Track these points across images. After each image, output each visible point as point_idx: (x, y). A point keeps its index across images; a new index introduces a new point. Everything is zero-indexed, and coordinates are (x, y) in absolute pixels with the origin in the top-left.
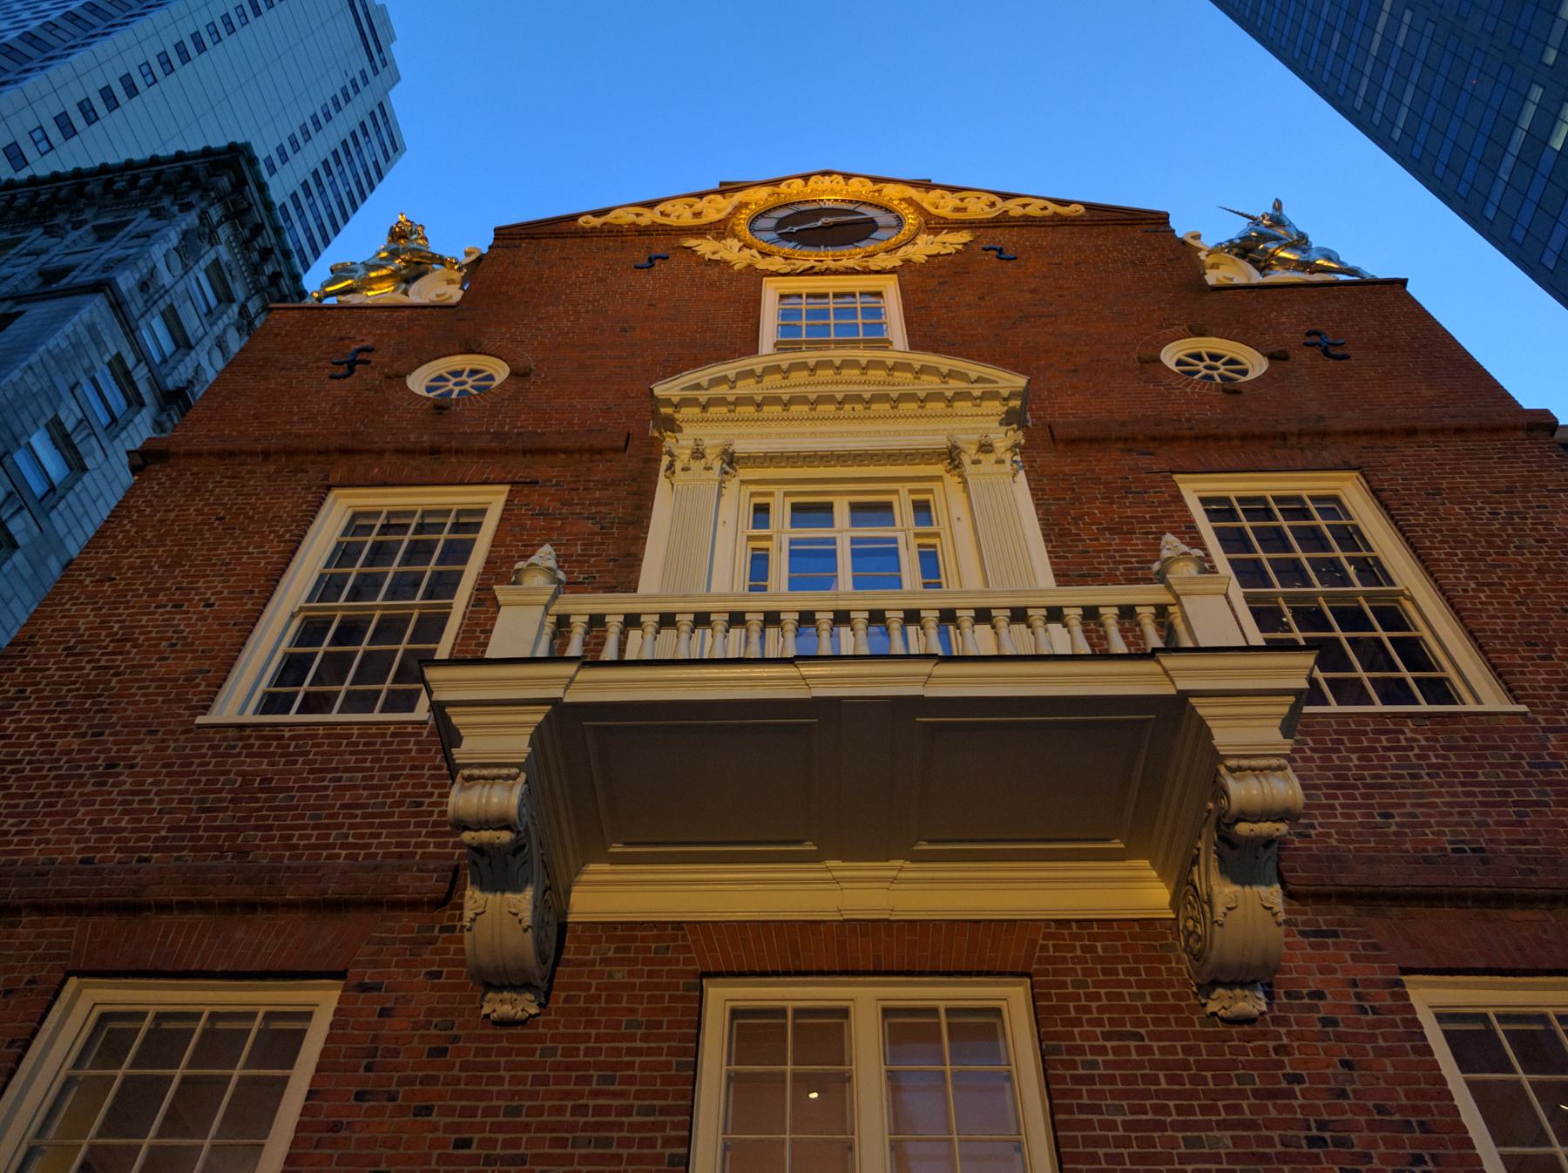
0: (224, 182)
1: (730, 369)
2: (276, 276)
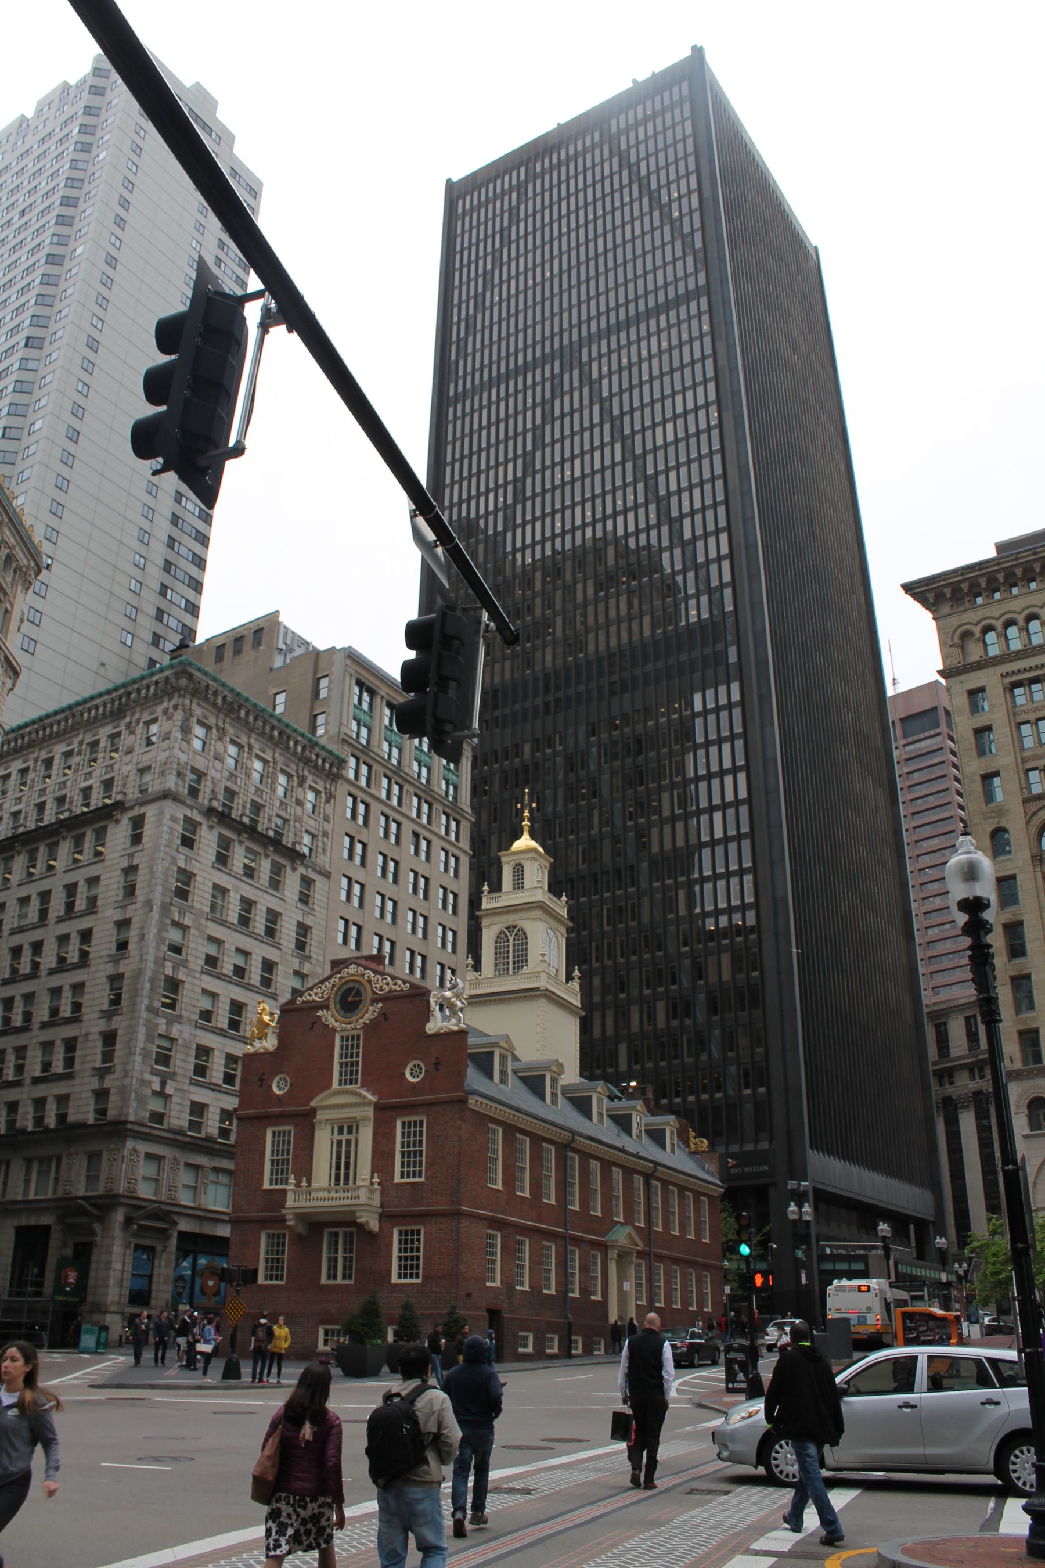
0: (183, 682)
1: (322, 1095)
2: (224, 698)
